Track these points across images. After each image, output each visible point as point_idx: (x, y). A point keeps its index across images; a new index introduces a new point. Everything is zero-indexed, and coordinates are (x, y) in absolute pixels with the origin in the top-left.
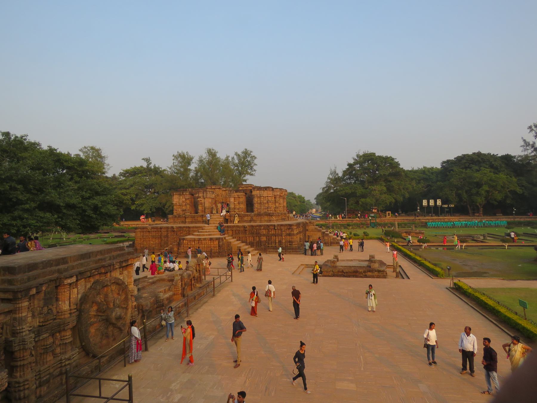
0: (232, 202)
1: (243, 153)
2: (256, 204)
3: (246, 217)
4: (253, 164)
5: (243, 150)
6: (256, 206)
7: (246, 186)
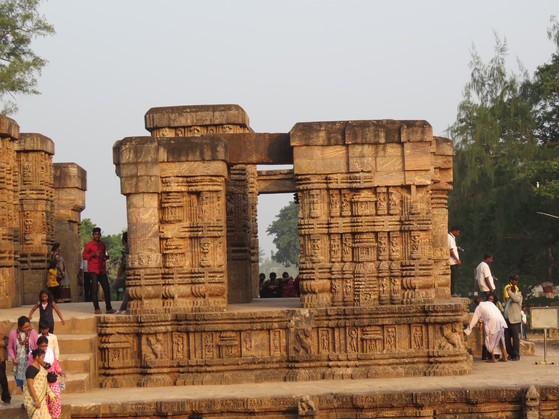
0: (147, 227)
2: (323, 244)
3: (258, 339)
4: (29, 24)
6: (321, 257)
7: (207, 118)
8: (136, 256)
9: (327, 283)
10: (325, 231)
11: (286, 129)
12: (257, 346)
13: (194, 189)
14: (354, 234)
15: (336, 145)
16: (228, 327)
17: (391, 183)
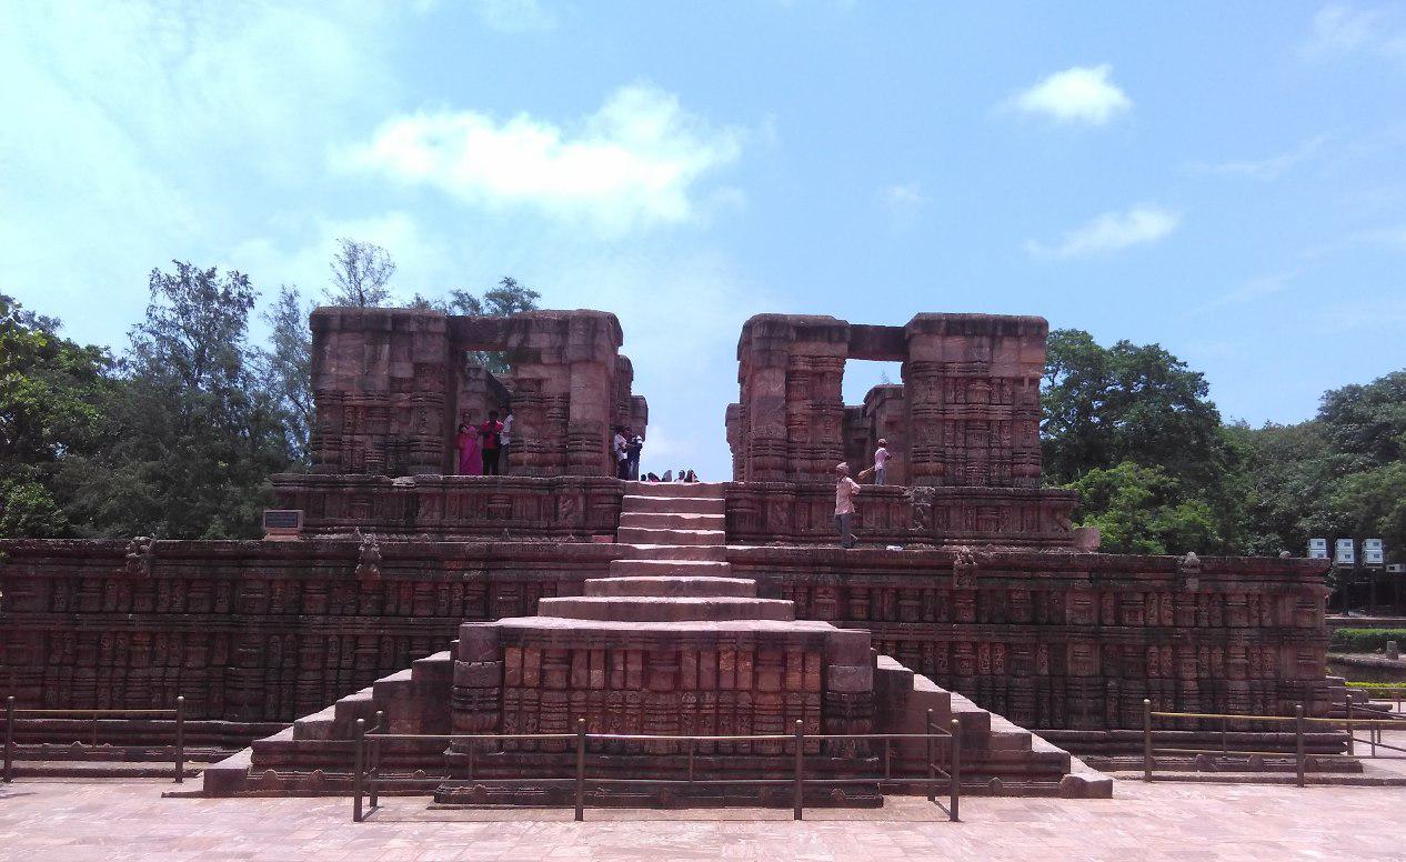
1: (491, 296)
5: (497, 285)
11: (900, 319)
13: (819, 369)
14: (967, 421)
15: (956, 334)
17: (1006, 374)
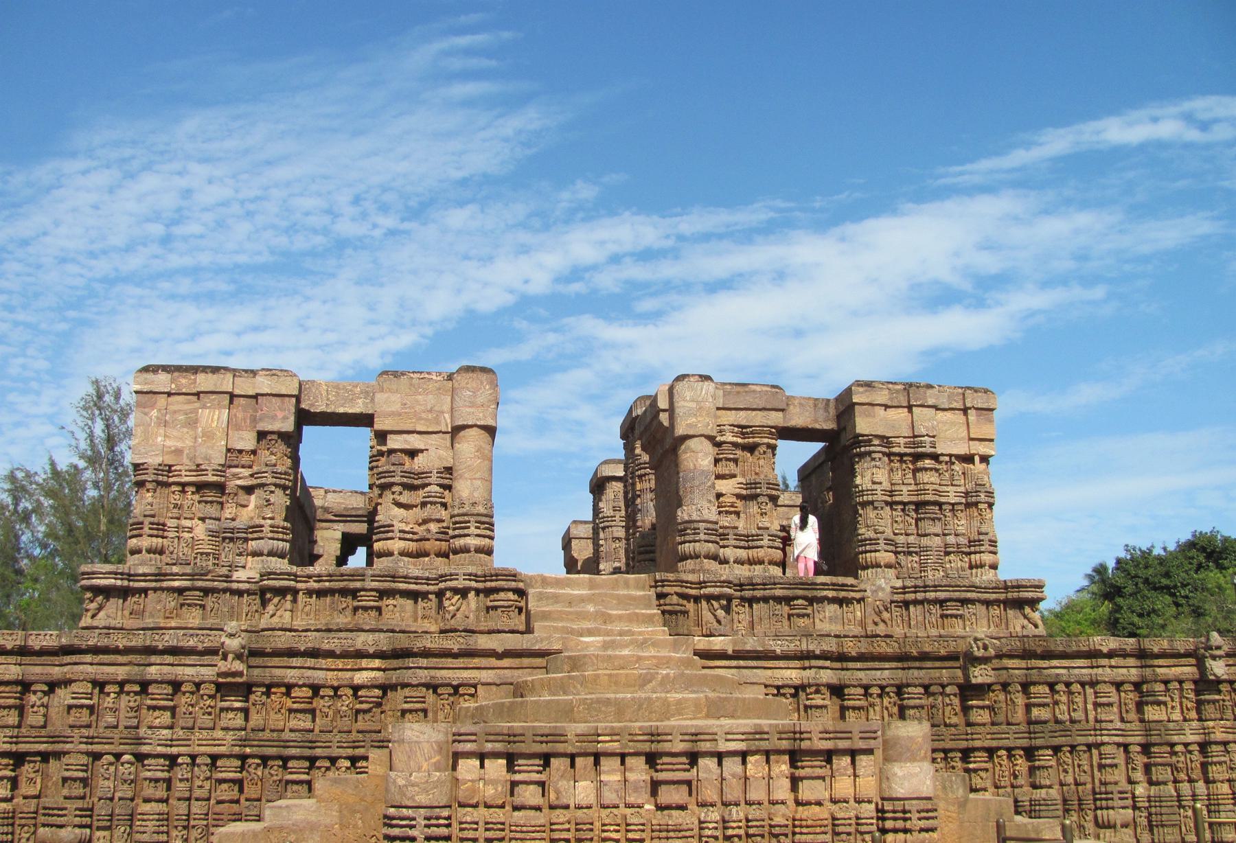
8: (694, 507)
9: (890, 557)
10: (889, 499)
12: (830, 618)
16: (800, 592)
17: (955, 451)
